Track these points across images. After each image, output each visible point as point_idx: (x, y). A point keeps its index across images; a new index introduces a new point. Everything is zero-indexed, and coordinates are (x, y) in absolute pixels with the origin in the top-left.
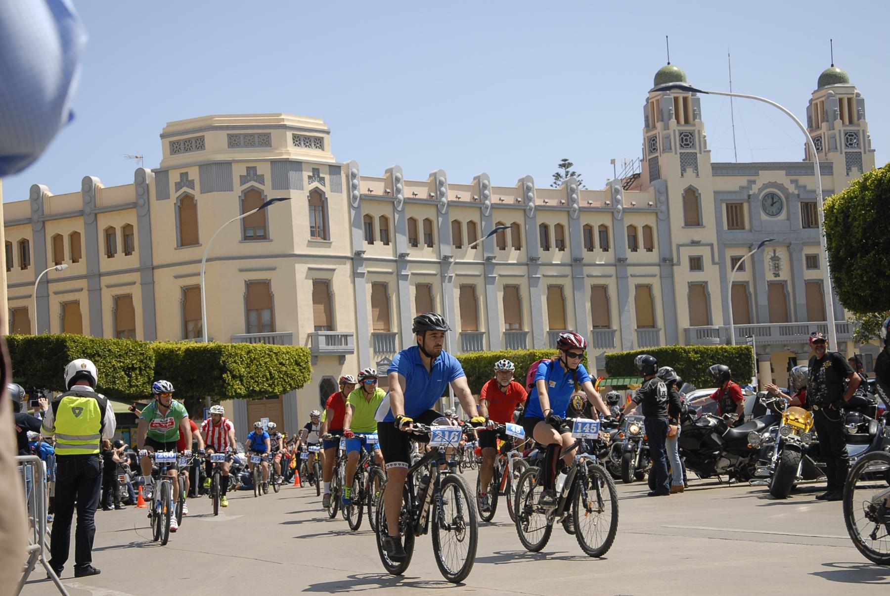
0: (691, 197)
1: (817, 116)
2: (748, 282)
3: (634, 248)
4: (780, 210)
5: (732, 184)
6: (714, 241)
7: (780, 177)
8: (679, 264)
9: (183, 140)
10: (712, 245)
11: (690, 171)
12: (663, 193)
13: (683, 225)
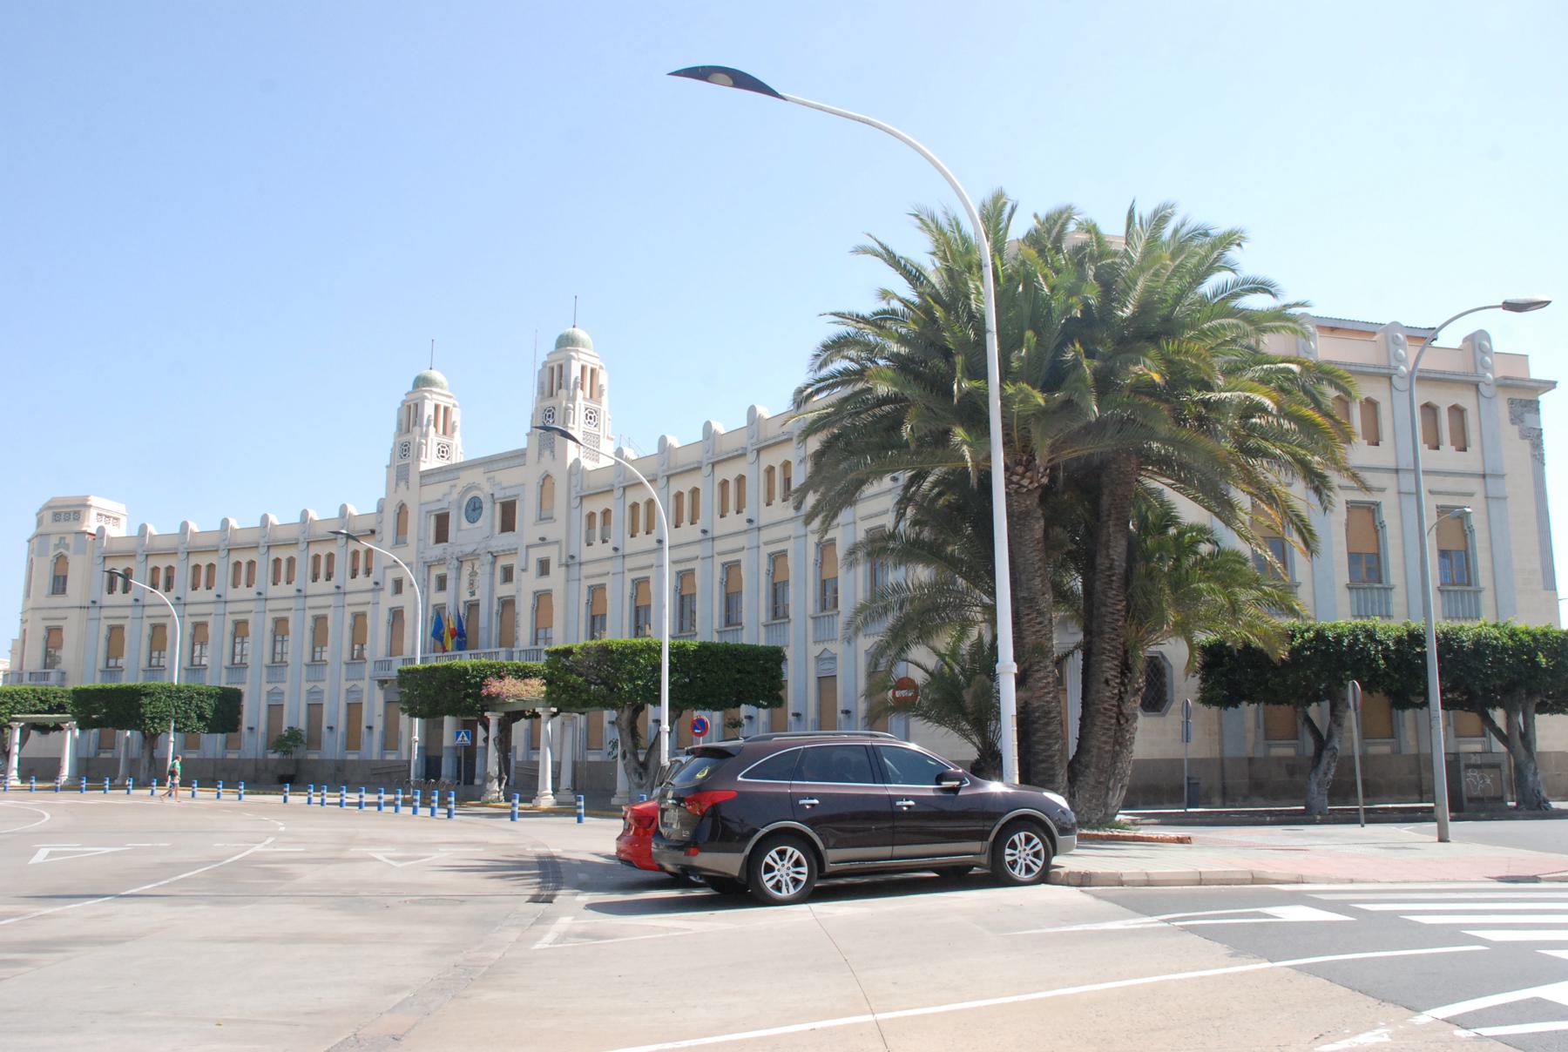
6: (413, 558)
7: (476, 476)
11: (402, 484)
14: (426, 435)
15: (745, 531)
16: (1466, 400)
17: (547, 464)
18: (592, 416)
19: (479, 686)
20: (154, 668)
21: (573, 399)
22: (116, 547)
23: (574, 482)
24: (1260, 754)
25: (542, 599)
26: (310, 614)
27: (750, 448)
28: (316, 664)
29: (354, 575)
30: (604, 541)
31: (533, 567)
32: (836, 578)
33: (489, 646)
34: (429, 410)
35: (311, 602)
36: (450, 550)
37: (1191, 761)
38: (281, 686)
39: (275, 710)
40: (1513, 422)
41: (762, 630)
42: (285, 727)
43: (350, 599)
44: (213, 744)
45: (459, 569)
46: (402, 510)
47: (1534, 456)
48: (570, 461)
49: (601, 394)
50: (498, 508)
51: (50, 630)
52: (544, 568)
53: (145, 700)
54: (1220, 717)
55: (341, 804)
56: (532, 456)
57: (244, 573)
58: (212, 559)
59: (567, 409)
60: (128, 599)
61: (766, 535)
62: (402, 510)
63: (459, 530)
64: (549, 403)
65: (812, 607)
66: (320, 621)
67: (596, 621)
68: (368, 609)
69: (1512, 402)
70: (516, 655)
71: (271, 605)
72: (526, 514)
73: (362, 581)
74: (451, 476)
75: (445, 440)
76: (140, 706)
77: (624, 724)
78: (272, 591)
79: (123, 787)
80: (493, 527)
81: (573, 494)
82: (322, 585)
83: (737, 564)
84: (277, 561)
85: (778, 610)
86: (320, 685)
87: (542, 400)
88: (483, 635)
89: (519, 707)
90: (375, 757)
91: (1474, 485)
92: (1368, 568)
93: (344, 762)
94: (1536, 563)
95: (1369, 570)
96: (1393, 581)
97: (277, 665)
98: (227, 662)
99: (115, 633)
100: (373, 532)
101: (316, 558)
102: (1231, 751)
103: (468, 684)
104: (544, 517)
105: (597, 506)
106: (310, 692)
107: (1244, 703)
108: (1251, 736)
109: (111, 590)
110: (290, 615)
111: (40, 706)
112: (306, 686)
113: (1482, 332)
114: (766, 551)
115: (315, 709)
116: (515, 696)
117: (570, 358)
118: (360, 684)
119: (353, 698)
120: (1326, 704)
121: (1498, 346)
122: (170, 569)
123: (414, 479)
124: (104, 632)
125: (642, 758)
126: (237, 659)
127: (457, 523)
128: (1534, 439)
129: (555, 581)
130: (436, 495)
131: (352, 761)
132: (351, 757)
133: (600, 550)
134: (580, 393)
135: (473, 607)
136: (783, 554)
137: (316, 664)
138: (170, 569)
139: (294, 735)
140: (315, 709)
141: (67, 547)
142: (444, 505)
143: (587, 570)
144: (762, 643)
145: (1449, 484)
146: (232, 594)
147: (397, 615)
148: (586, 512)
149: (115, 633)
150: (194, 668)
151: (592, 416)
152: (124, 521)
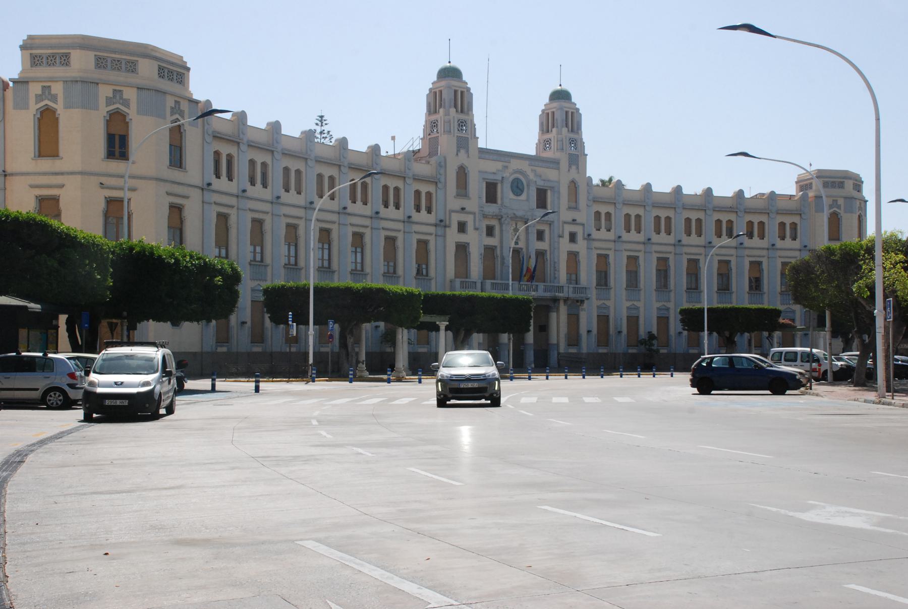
0: (462, 173)
1: (548, 122)
2: (496, 247)
3: (418, 209)
4: (522, 191)
5: (492, 166)
6: (476, 210)
7: (525, 166)
8: (449, 227)
9: (42, 53)
10: (474, 214)
11: (462, 151)
12: (442, 165)
13: (455, 194)
25: (573, 257)
51: (110, 201)
52: (573, 238)
66: (391, 241)
104: (574, 207)
127: (505, 193)
145: (628, 246)
147: (462, 249)
149: (223, 219)
150: (325, 269)
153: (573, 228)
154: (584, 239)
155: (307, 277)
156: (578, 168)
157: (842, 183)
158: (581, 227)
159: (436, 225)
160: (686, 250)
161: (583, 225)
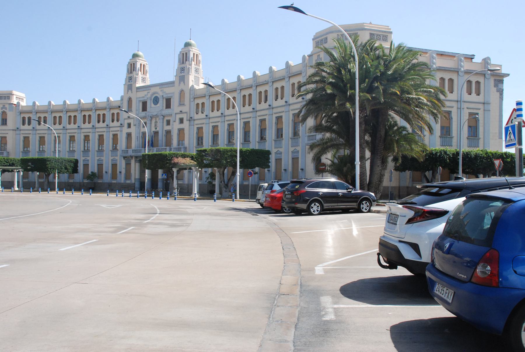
4: (158, 102)
7: (157, 89)
11: (130, 91)
14: (138, 74)
15: (252, 112)
16: (481, 80)
17: (182, 86)
18: (197, 71)
19: (171, 160)
20: (41, 152)
21: (191, 65)
22: (25, 109)
23: (192, 93)
24: (410, 186)
25: (181, 131)
26: (97, 134)
27: (254, 85)
28: (100, 151)
29: (113, 121)
30: (202, 113)
31: (178, 121)
32: (282, 128)
33: (162, 146)
34: (138, 66)
35: (97, 130)
36: (147, 114)
37: (392, 187)
38: (88, 158)
39: (86, 166)
40: (495, 87)
41: (257, 144)
42: (90, 173)
43: (111, 129)
44: (65, 177)
45: (151, 120)
46: (130, 100)
47: (500, 97)
48: (190, 85)
49: (199, 63)
50: (165, 100)
52: (181, 121)
53: (48, 163)
54: (399, 175)
55: (130, 196)
56: (177, 83)
57: (72, 120)
58: (61, 114)
59: (189, 68)
60: (30, 127)
61: (259, 113)
62: (130, 100)
63: (151, 107)
64: (183, 66)
65: (274, 137)
66: (101, 137)
67: (200, 140)
68: (118, 133)
69: (495, 80)
70: (172, 149)
71: (83, 131)
72: (175, 102)
73: (116, 123)
74: (147, 89)
75: (144, 76)
76: (47, 164)
77: (221, 173)
78: (83, 126)
79: (38, 191)
80: (163, 107)
81: (192, 97)
82: (101, 124)
83: (249, 122)
84: (84, 116)
85: (262, 138)
86: (102, 158)
87: (180, 64)
88: (160, 142)
89: (184, 167)
90: (123, 181)
91: (481, 106)
92: (446, 131)
93: (111, 183)
94: (498, 132)
95: (446, 132)
96: (453, 135)
97: (86, 151)
98: (68, 149)
99: (26, 140)
100: (119, 107)
101: (99, 115)
102: (402, 185)
103: (167, 160)
104: (181, 104)
105: (200, 101)
106: (98, 160)
107: (407, 171)
108: (408, 180)
109: (24, 124)
110: (90, 134)
111: (6, 164)
112: (97, 158)
113: (488, 57)
114: (258, 119)
115: (100, 166)
116: (184, 164)
117: (189, 51)
118: (116, 158)
119: (114, 162)
120: (431, 172)
121: (493, 62)
122: (45, 118)
123: (134, 90)
124: (22, 139)
125: (226, 183)
126: (71, 149)
128: (501, 92)
129: (186, 125)
130: (141, 94)
131: (114, 183)
132: (113, 182)
133: (201, 116)
134: (193, 63)
135: (156, 133)
136: (265, 120)
137: (100, 151)
138: (45, 118)
139: (93, 174)
140: (100, 166)
141: (6, 109)
142: (145, 98)
143: (196, 122)
144: (257, 148)
146: (68, 126)
147: (129, 135)
148: (196, 103)
149: (26, 140)
151: (197, 71)
152: (25, 100)
153: (181, 116)
154: (187, 120)
155: (237, 146)
156: (184, 82)
157: (326, 38)
158: (186, 114)
159: (120, 127)
160: (227, 118)
161: (186, 113)
